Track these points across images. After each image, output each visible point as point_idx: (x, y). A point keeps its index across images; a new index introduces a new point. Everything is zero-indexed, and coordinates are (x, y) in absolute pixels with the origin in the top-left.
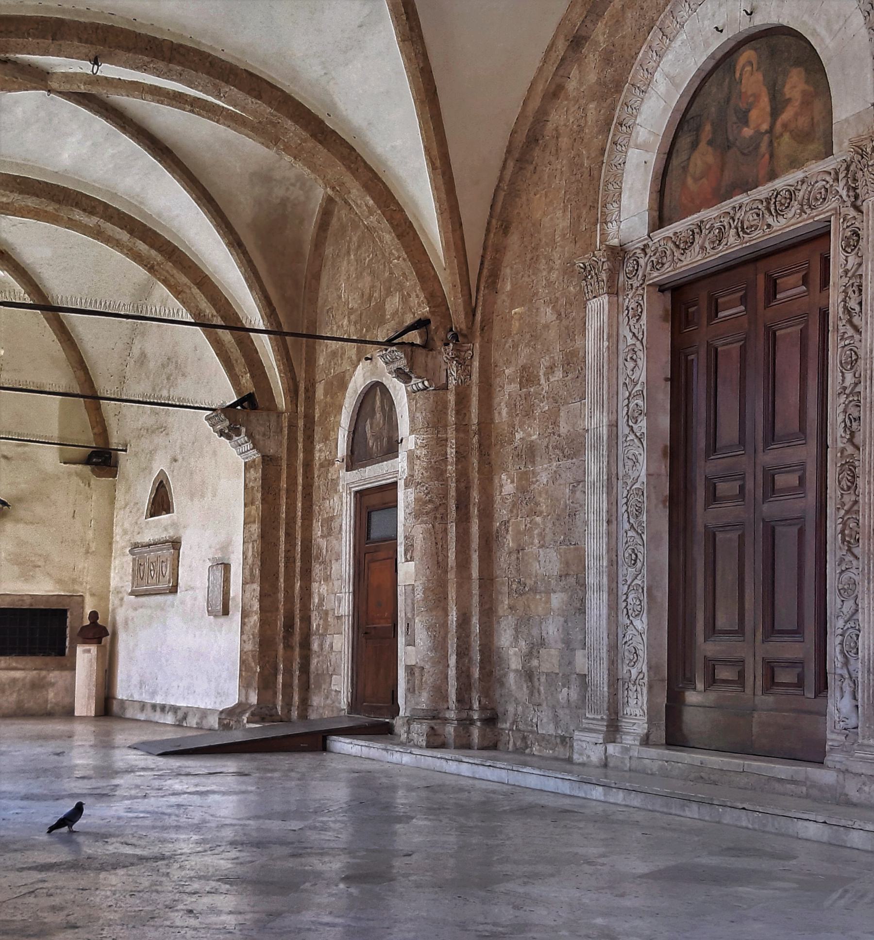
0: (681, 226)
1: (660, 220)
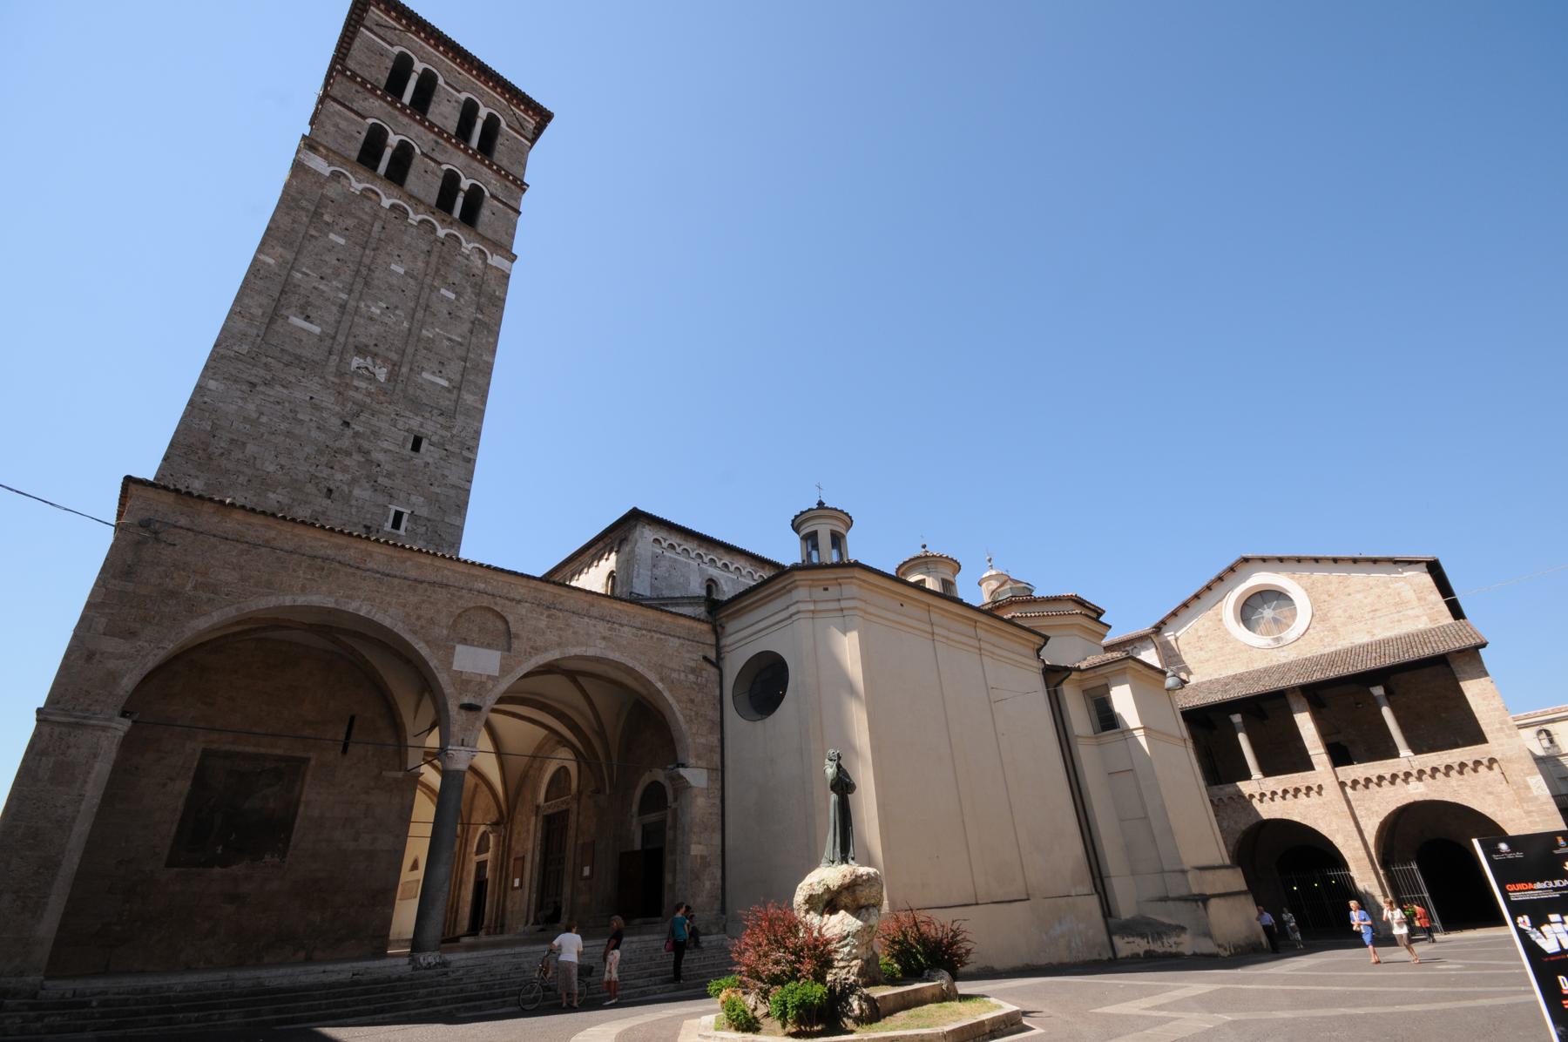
0: (549, 803)
1: (546, 800)
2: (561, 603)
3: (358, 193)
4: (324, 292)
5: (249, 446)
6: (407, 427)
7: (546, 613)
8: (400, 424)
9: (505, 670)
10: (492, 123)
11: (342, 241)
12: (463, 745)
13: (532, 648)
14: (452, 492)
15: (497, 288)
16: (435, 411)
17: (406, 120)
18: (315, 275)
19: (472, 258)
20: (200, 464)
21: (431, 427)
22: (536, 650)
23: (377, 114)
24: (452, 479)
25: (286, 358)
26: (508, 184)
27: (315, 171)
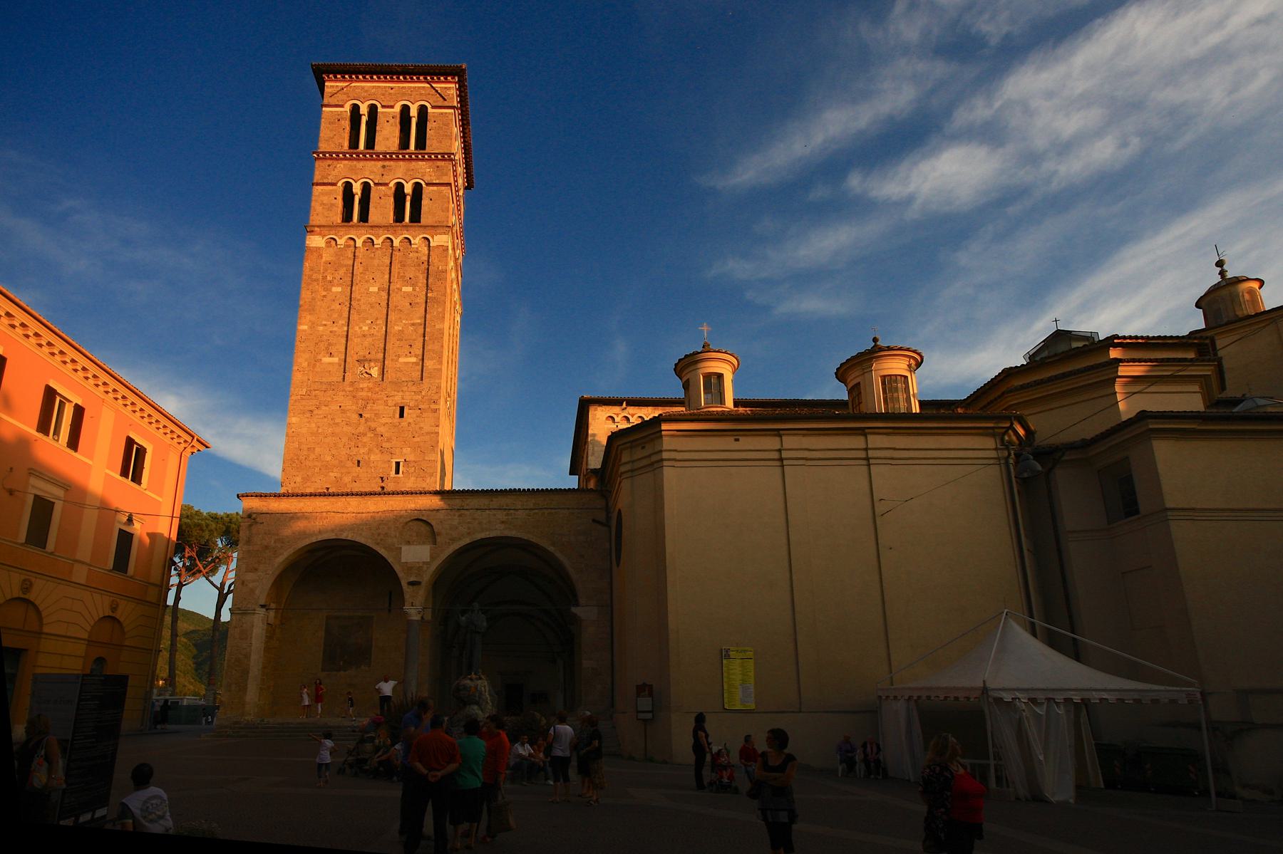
2: (467, 505)
3: (342, 247)
4: (336, 332)
5: (316, 449)
6: (394, 402)
7: (457, 514)
8: (390, 403)
9: (433, 558)
10: (423, 111)
11: (339, 289)
12: (412, 606)
13: (450, 540)
14: (427, 438)
15: (440, 263)
16: (409, 384)
17: (360, 164)
18: (329, 323)
19: (420, 249)
20: (297, 468)
21: (407, 398)
22: (453, 540)
23: (344, 174)
24: (427, 428)
25: (324, 387)
26: (439, 163)
27: (316, 247)
